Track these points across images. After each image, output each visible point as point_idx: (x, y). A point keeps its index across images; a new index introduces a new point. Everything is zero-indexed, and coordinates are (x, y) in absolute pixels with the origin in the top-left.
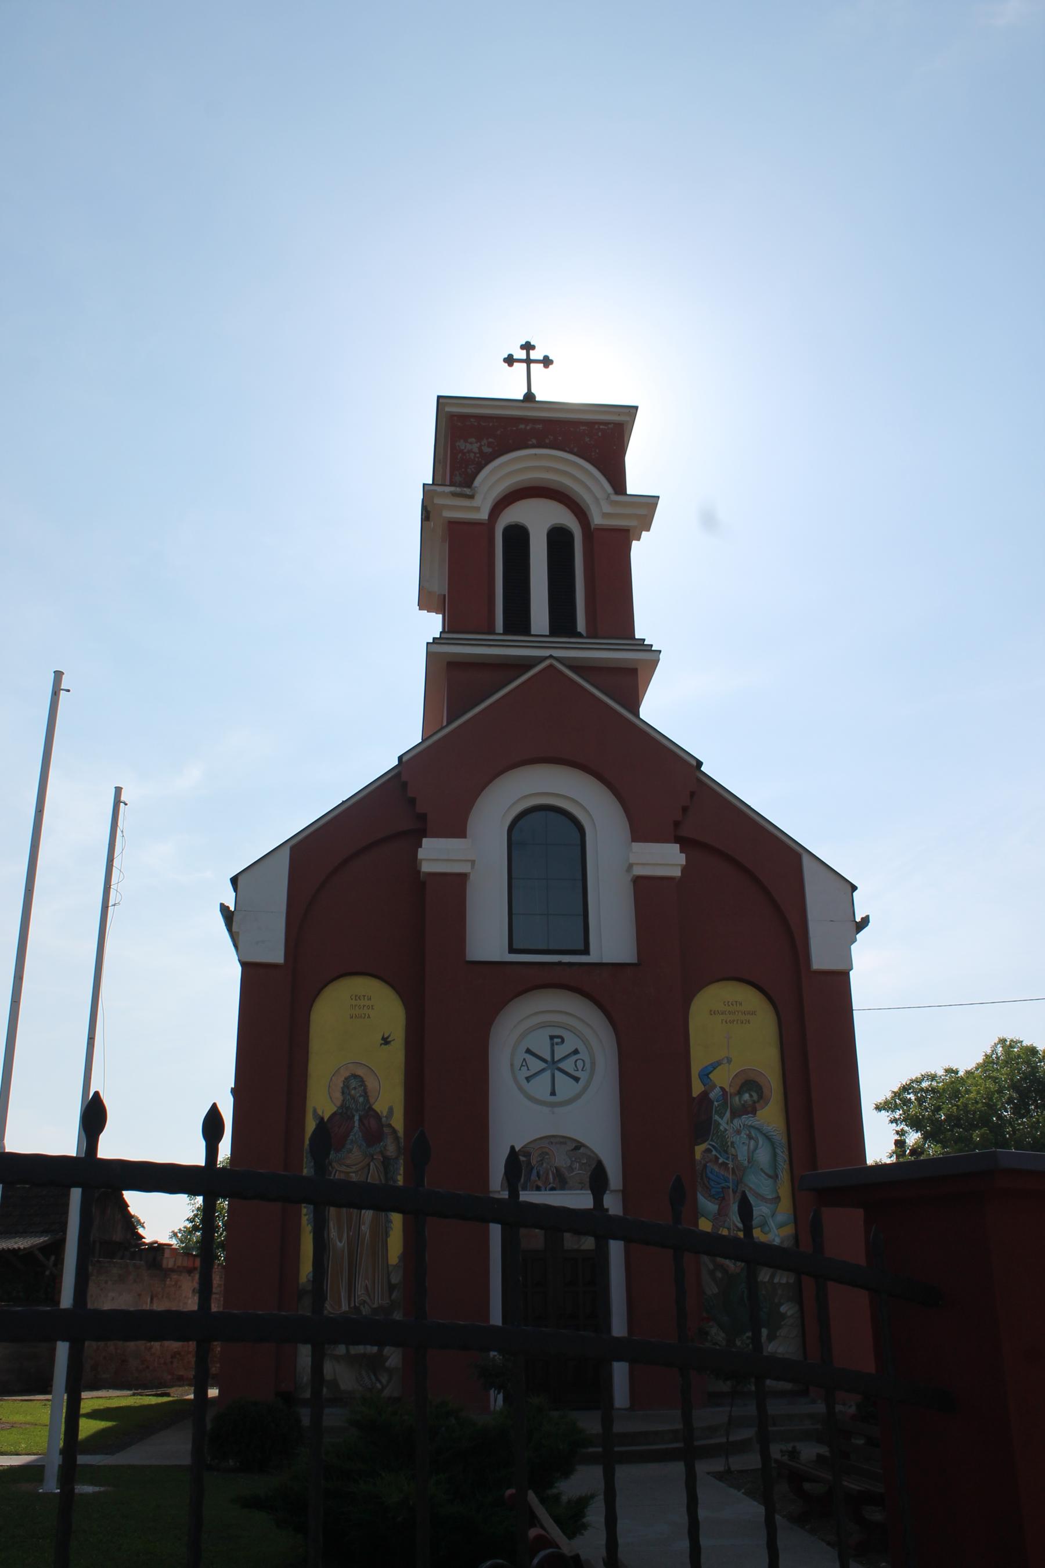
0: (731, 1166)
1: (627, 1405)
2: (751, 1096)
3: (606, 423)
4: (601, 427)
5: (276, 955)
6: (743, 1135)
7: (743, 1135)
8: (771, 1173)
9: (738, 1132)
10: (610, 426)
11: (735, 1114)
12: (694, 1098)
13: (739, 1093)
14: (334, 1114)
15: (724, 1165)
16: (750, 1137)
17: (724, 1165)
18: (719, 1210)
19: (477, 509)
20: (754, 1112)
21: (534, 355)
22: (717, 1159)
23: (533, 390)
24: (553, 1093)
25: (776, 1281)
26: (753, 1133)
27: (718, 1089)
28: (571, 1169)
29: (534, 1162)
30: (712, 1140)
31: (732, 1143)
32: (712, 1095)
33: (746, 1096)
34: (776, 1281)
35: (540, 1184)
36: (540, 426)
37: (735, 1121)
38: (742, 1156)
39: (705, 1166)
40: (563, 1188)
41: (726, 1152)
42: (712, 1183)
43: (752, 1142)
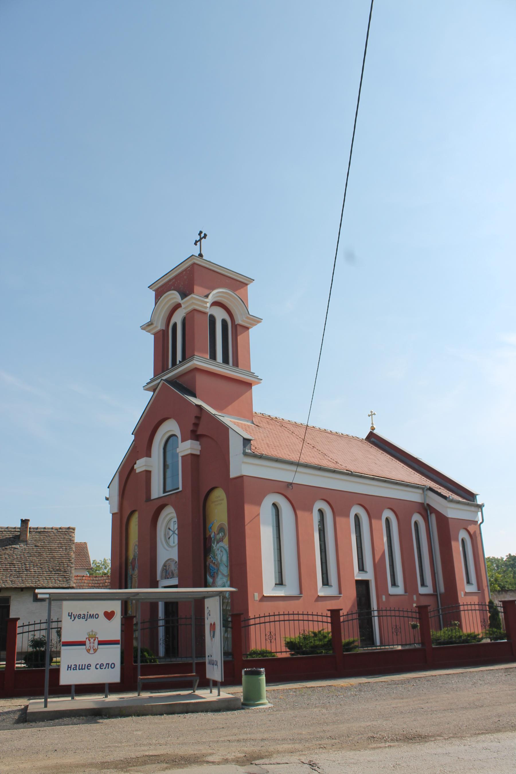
0: (216, 563)
1: (164, 655)
2: (222, 534)
3: (189, 267)
4: (189, 269)
5: (116, 510)
6: (219, 551)
7: (219, 551)
8: (226, 565)
9: (218, 550)
10: (191, 267)
11: (218, 543)
12: (207, 538)
13: (218, 534)
14: (133, 559)
15: (214, 563)
16: (221, 551)
17: (214, 563)
18: (213, 581)
19: (156, 327)
20: (222, 541)
21: (202, 235)
22: (213, 561)
23: (202, 252)
24: (174, 543)
25: (227, 609)
26: (223, 549)
27: (213, 533)
28: (175, 570)
29: (167, 569)
30: (212, 554)
31: (217, 554)
32: (212, 536)
33: (221, 534)
34: (227, 609)
35: (168, 576)
36: (174, 280)
37: (218, 545)
38: (219, 560)
39: (209, 564)
40: (173, 578)
41: (215, 558)
42: (211, 571)
43: (222, 553)
